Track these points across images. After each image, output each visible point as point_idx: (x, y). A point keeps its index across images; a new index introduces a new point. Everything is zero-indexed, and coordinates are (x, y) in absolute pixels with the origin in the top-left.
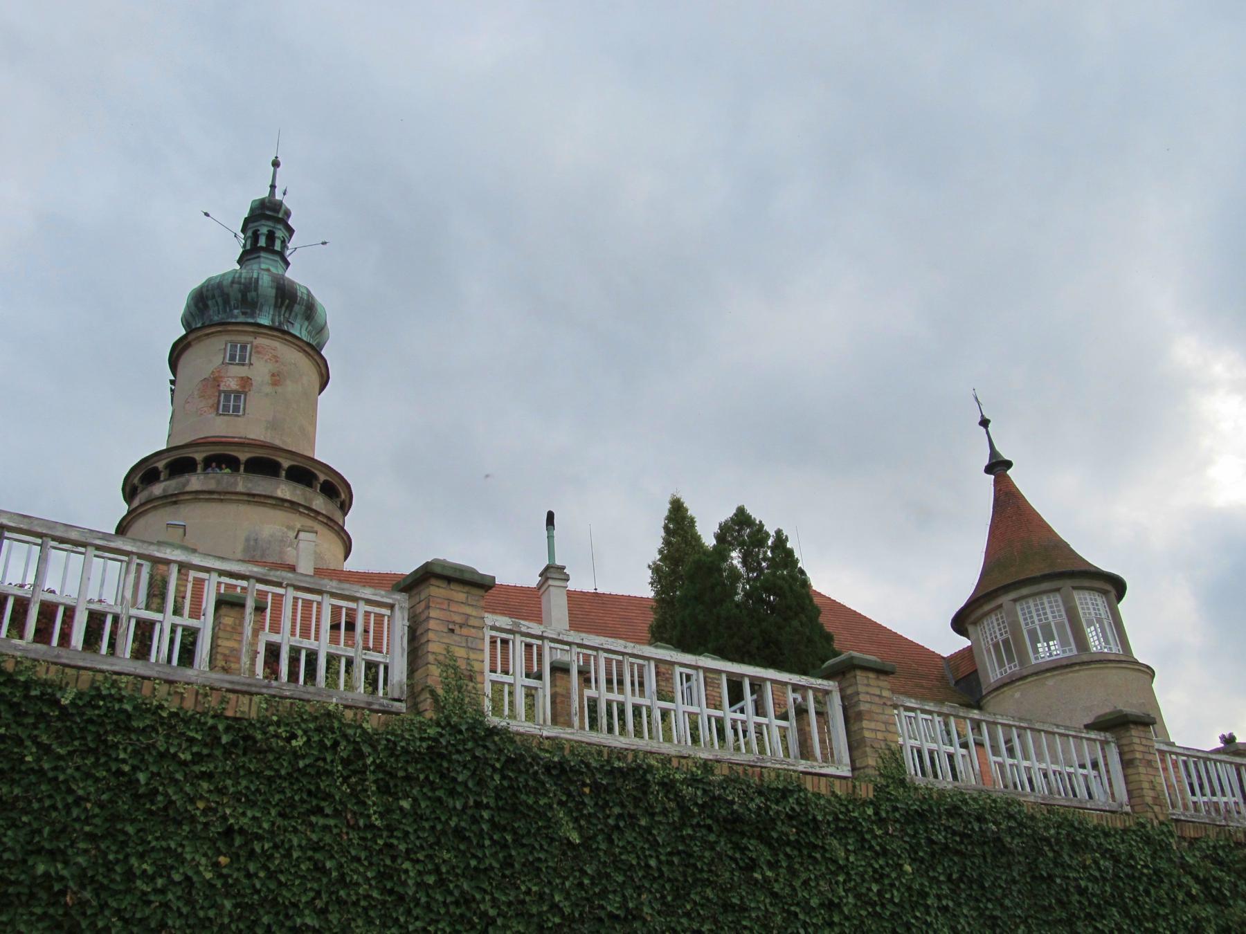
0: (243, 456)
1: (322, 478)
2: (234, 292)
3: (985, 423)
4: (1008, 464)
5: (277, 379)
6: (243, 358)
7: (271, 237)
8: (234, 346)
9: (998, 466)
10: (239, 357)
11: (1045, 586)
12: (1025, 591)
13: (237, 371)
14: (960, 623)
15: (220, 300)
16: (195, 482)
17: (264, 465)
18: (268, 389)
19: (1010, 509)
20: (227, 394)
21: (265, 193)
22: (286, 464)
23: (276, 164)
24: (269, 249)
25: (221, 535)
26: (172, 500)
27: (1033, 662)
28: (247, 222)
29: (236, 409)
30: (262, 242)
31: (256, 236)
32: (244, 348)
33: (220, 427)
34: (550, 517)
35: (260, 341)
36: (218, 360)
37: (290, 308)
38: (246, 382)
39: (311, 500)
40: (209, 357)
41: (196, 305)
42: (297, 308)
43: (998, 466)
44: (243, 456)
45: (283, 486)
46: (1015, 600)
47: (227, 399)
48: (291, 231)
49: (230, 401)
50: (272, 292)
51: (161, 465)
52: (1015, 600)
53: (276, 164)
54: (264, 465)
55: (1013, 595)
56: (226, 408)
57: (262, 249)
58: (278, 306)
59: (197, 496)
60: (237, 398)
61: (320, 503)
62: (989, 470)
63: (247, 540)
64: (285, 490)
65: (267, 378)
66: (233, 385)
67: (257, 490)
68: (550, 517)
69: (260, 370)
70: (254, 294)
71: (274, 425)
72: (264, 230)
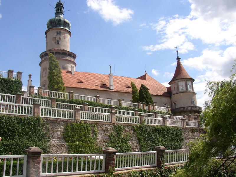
0: (61, 52)
2: (57, 22)
3: (177, 51)
4: (180, 59)
6: (59, 34)
7: (61, 10)
8: (57, 32)
9: (178, 59)
11: (183, 80)
12: (180, 80)
14: (169, 83)
15: (54, 23)
19: (179, 69)
20: (57, 40)
22: (68, 53)
29: (59, 43)
32: (59, 32)
37: (66, 24)
39: (71, 59)
40: (53, 33)
41: (50, 23)
42: (67, 24)
44: (61, 52)
45: (67, 57)
46: (178, 82)
47: (57, 41)
50: (63, 22)
52: (178, 82)
55: (178, 81)
56: (57, 43)
57: (59, 12)
60: (59, 41)
61: (72, 60)
62: (177, 59)
63: (63, 66)
64: (68, 58)
70: (60, 22)
72: (60, 9)
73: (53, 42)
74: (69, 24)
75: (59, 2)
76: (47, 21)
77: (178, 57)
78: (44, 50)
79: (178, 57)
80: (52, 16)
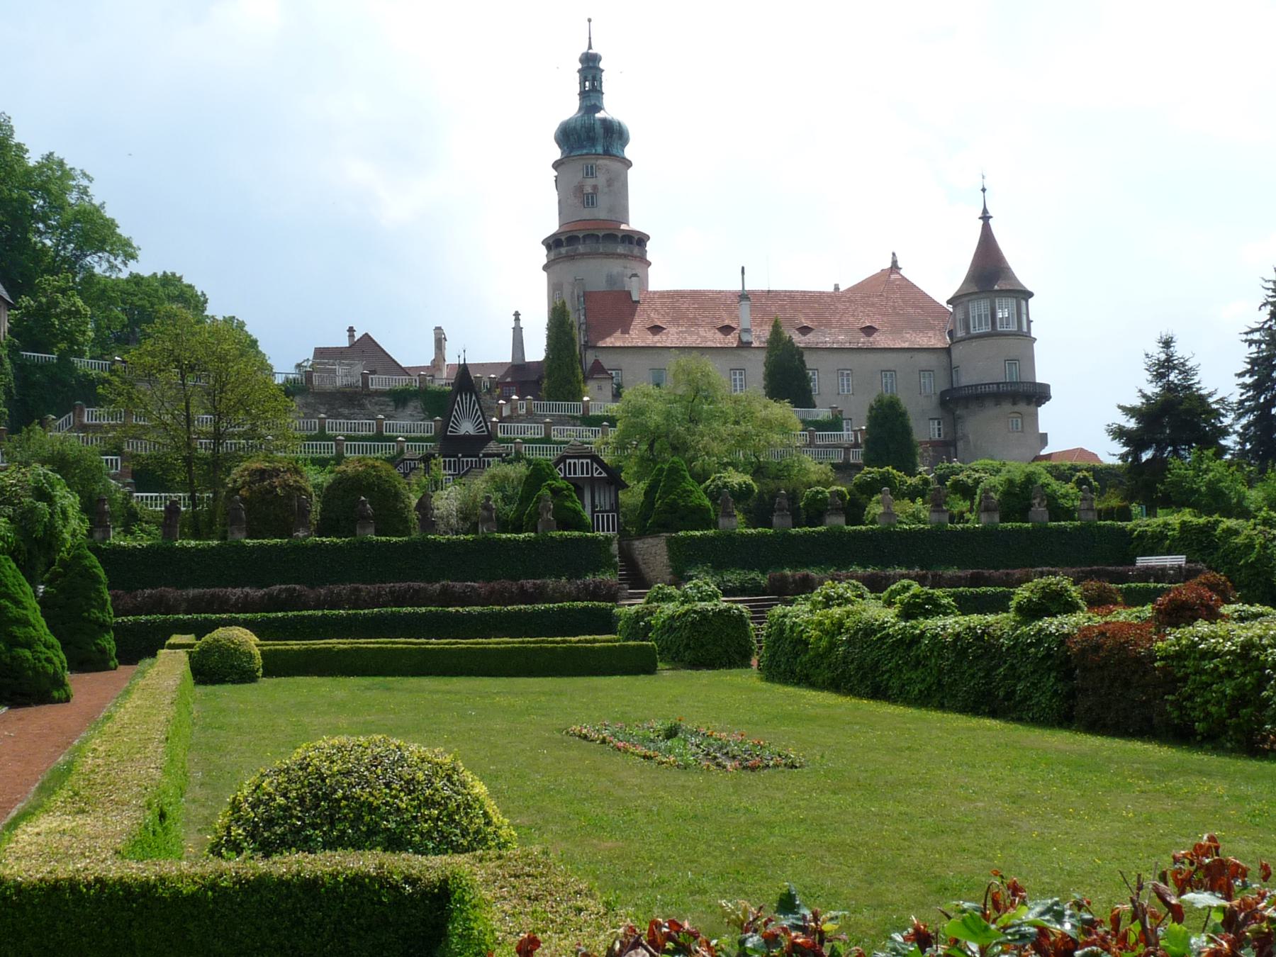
0: (601, 234)
3: (984, 190)
9: (985, 217)
10: (590, 172)
13: (590, 182)
16: (581, 248)
18: (606, 190)
21: (585, 49)
23: (590, 20)
25: (597, 272)
27: (972, 331)
35: (600, 162)
38: (595, 187)
43: (985, 217)
44: (601, 234)
49: (589, 200)
50: (601, 131)
51: (563, 238)
61: (636, 251)
66: (589, 190)
69: (601, 180)
77: (985, 211)
78: (551, 225)
79: (985, 211)
80: (569, 107)
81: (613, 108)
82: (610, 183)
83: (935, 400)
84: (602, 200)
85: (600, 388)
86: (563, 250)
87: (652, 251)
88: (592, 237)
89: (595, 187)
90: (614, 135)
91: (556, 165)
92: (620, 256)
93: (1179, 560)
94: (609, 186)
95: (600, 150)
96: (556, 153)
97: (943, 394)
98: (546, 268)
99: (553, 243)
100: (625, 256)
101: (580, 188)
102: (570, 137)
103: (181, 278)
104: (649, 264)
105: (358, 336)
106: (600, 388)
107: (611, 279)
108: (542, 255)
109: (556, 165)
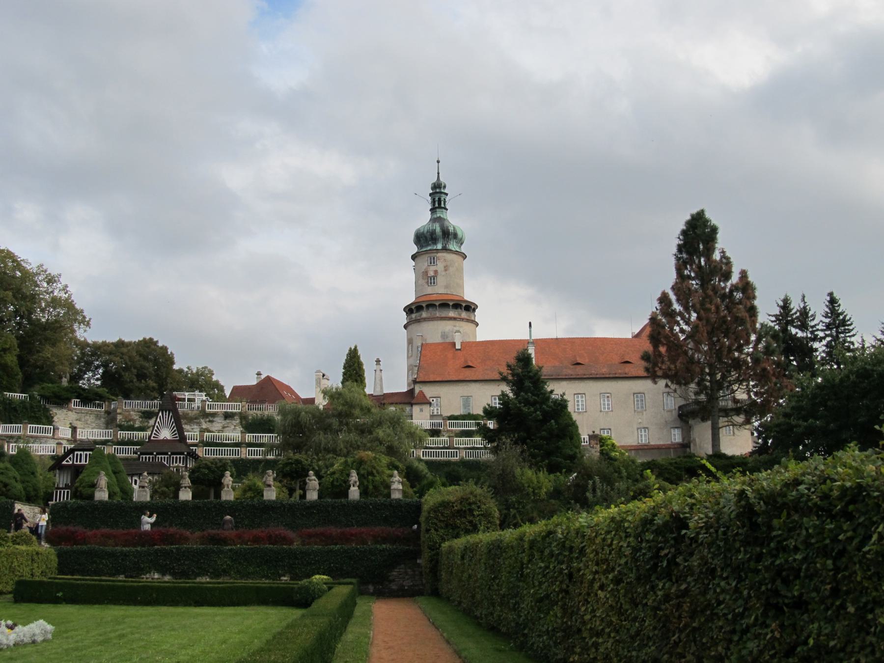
0: (437, 304)
1: (464, 305)
2: (429, 236)
5: (446, 268)
7: (440, 200)
10: (433, 262)
16: (424, 314)
17: (444, 305)
18: (444, 273)
22: (451, 304)
23: (438, 162)
24: (440, 207)
25: (434, 331)
26: (418, 321)
28: (430, 195)
30: (437, 205)
31: (434, 202)
33: (429, 290)
34: (530, 323)
35: (439, 255)
36: (426, 264)
37: (448, 237)
38: (436, 272)
39: (460, 315)
40: (424, 262)
44: (437, 304)
48: (447, 194)
49: (431, 280)
50: (441, 234)
51: (413, 307)
53: (438, 162)
54: (444, 305)
58: (444, 238)
59: (425, 320)
61: (464, 314)
64: (452, 313)
65: (443, 269)
66: (431, 274)
67: (443, 315)
68: (530, 323)
69: (440, 266)
71: (447, 287)
73: (422, 282)
74: (455, 236)
75: (434, 184)
76: (412, 237)
78: (411, 299)
80: (423, 219)
81: (454, 219)
82: (446, 268)
83: (675, 414)
84: (441, 280)
85: (421, 410)
86: (413, 316)
87: (478, 315)
88: (431, 305)
89: (436, 272)
90: (448, 235)
91: (414, 257)
92: (451, 319)
93: (780, 532)
94: (446, 270)
95: (439, 246)
96: (415, 249)
97: (680, 408)
98: (405, 327)
99: (409, 310)
100: (455, 319)
101: (426, 273)
102: (423, 239)
103: (157, 342)
104: (477, 325)
105: (263, 377)
106: (421, 410)
107: (444, 335)
108: (403, 318)
109: (414, 257)
